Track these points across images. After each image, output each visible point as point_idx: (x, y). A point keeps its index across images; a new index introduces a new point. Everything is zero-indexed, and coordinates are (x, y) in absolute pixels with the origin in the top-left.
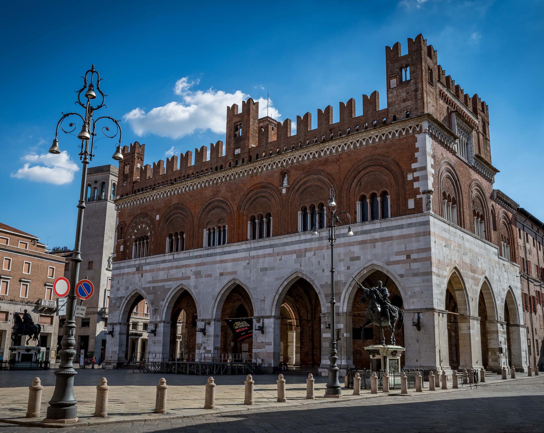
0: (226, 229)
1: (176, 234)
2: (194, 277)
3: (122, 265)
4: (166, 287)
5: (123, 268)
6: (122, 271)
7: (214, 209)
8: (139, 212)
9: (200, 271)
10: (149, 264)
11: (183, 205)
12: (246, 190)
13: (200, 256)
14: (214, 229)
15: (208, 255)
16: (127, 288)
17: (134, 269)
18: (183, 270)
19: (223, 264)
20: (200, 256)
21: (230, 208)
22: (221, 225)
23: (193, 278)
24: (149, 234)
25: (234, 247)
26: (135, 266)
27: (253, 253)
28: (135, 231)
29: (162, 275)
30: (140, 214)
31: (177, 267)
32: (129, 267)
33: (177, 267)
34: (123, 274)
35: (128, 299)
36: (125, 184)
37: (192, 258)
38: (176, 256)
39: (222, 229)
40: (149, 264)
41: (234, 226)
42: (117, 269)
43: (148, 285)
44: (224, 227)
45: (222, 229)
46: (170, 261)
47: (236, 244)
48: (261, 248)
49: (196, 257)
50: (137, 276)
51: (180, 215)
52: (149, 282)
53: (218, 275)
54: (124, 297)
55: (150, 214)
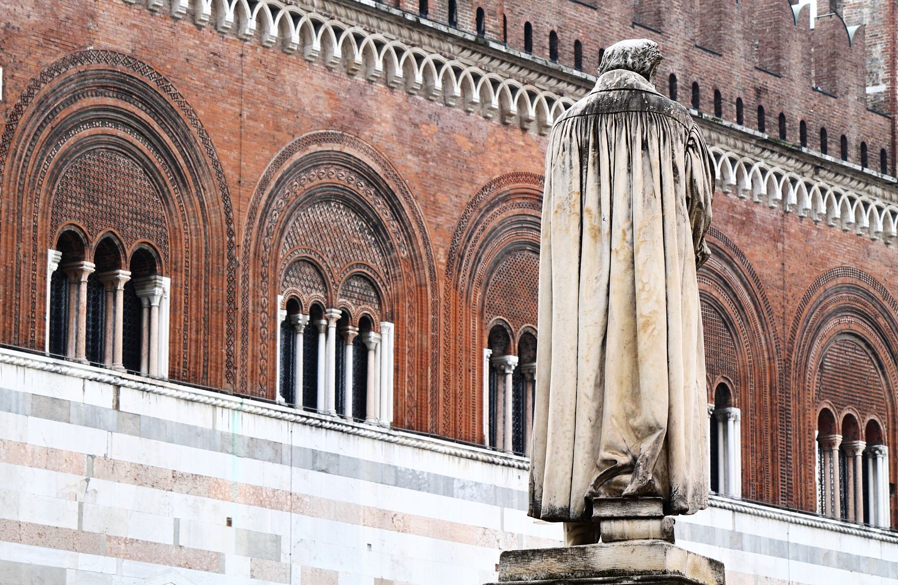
0: (384, 340)
1: (108, 255)
2: (245, 564)
7: (327, 201)
9: (277, 539)
11: (162, 81)
12: (482, 180)
13: (276, 452)
14: (317, 311)
15: (319, 462)
18: (179, 503)
19: (392, 536)
20: (276, 452)
21: (410, 238)
22: (357, 312)
25: (435, 458)
31: (141, 476)
33: (141, 476)
37: (226, 444)
38: (131, 400)
39: (353, 331)
41: (435, 341)
44: (366, 324)
45: (353, 331)
46: (91, 418)
49: (253, 448)
51: (139, 142)
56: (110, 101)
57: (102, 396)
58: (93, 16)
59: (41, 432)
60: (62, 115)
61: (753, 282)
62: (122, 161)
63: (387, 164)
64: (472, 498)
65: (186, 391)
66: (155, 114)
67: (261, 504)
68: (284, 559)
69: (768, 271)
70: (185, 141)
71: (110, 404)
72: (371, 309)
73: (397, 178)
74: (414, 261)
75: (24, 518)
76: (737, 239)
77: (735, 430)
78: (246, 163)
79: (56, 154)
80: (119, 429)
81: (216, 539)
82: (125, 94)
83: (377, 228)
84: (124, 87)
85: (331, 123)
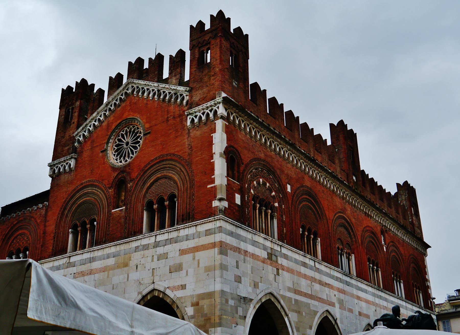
0: (353, 257)
3: (241, 232)
4: (312, 308)
5: (245, 240)
6: (243, 246)
8: (262, 156)
10: (286, 257)
11: (316, 194)
12: (364, 226)
14: (342, 250)
16: (256, 286)
17: (264, 254)
23: (337, 305)
24: (276, 205)
26: (265, 248)
27: (377, 301)
28: (255, 182)
29: (304, 285)
30: (264, 161)
32: (254, 243)
34: (246, 252)
35: (257, 307)
36: (234, 83)
37: (332, 277)
40: (286, 257)
42: (231, 234)
43: (289, 294)
46: (311, 268)
47: (366, 282)
48: (381, 297)
49: (337, 279)
50: (270, 268)
52: (289, 289)
53: (358, 314)
54: (251, 300)
55: (278, 171)
56: (308, 197)
57: (312, 263)
58: (304, 178)
59: (303, 270)
60: (300, 198)
61: (401, 254)
62: (310, 211)
63: (350, 220)
64: (370, 295)
65: (326, 264)
66: (315, 201)
67: (339, 292)
68: (344, 305)
69: (403, 253)
70: (320, 208)
71: (314, 265)
72: (349, 251)
73: (352, 223)
74: (356, 241)
75: (302, 290)
76: (398, 246)
77: (402, 285)
78: (330, 215)
79: (300, 207)
80: (315, 271)
81: (334, 300)
82: (310, 196)
83: (349, 233)
84: (310, 194)
85: (341, 209)
